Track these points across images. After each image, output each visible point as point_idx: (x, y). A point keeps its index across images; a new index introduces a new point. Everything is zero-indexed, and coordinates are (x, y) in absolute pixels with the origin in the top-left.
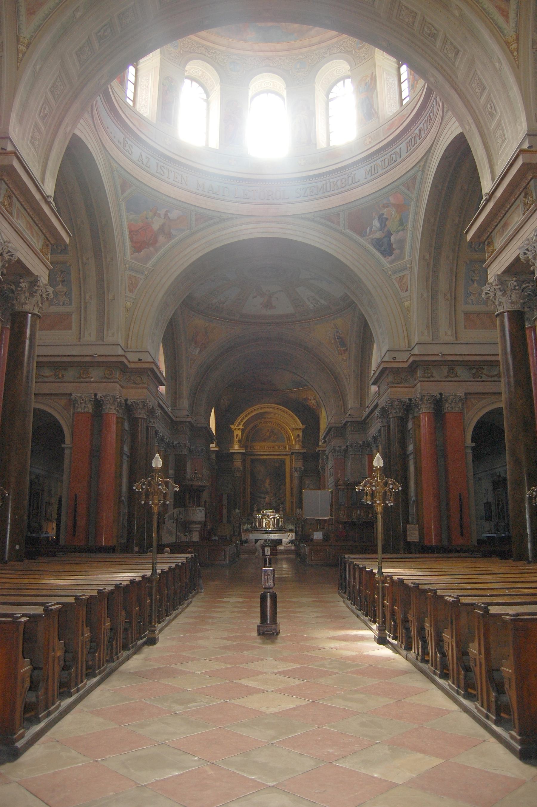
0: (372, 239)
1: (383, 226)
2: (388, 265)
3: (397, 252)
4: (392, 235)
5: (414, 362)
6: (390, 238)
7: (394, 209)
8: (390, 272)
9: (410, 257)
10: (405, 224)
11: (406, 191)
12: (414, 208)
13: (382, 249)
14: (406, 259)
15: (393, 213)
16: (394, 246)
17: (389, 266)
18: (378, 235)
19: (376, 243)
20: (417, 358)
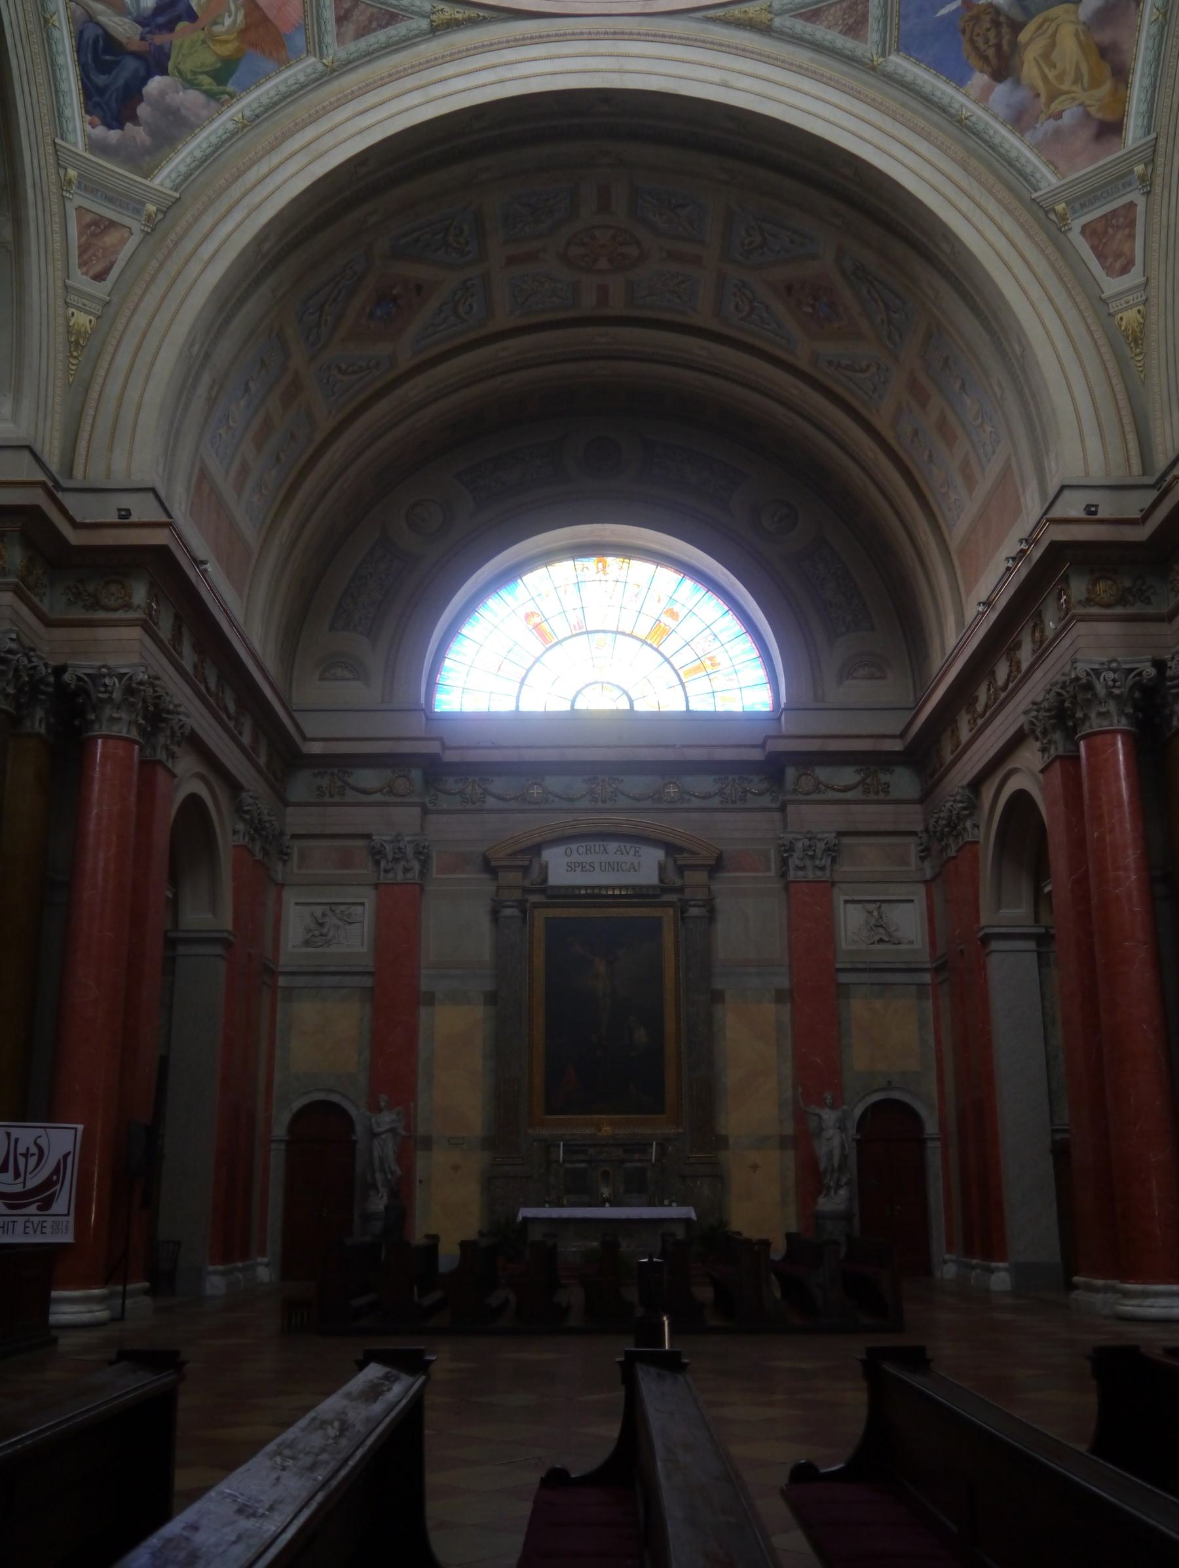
0: (91, 18)
1: (161, 20)
2: (80, 149)
3: (137, 133)
4: (164, 72)
5: (162, 554)
6: (149, 75)
7: (240, 17)
8: (72, 173)
9: (176, 190)
10: (230, 88)
11: (329, 14)
12: (302, 78)
13: (101, 80)
14: (156, 182)
15: (228, 21)
16: (143, 110)
17: (80, 149)
18: (123, 28)
19: (96, 41)
20: (174, 548)
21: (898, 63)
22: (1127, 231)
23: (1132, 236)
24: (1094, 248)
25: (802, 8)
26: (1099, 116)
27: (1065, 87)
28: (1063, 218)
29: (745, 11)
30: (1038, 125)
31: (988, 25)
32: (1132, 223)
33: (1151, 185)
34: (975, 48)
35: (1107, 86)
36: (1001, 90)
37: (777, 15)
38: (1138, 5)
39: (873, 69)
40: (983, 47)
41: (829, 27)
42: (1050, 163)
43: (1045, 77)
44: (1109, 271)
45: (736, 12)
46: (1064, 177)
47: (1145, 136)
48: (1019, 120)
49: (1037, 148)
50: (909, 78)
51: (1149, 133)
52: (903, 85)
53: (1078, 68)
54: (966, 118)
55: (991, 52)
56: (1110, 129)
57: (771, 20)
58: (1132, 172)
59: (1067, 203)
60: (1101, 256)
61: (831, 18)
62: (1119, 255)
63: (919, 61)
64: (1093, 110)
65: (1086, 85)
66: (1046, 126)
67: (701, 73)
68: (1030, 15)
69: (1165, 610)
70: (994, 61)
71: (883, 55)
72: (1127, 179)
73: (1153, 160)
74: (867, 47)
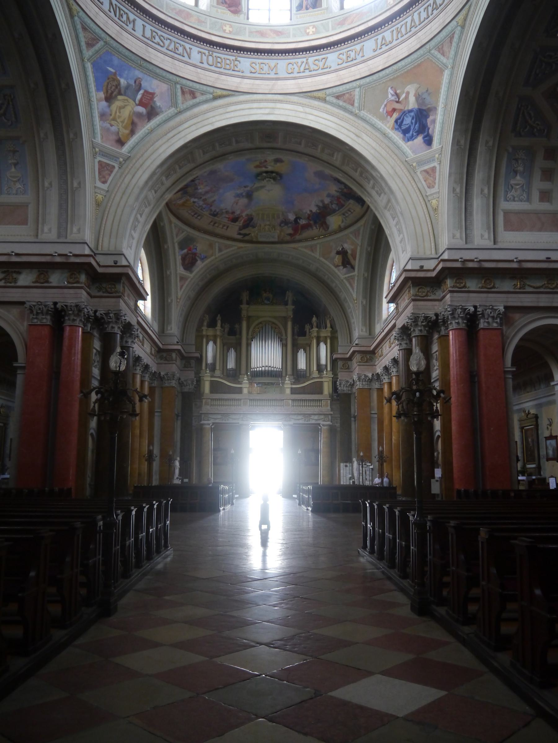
21: (89, 66)
22: (109, 172)
23: (110, 175)
24: (99, 169)
25: (84, 23)
26: (121, 136)
27: (119, 120)
28: (96, 153)
29: (73, 5)
30: (105, 122)
31: (114, 84)
32: (112, 172)
33: (122, 166)
34: (107, 86)
35: (127, 132)
36: (104, 103)
37: (78, 16)
38: (148, 122)
39: (83, 61)
40: (109, 88)
41: (84, 37)
42: (102, 135)
43: (116, 113)
44: (100, 179)
45: (71, 2)
46: (102, 143)
47: (127, 153)
48: (103, 116)
49: (102, 129)
50: (88, 74)
51: (129, 153)
52: (85, 75)
53: (125, 119)
54: (92, 101)
55: (110, 92)
56: (121, 142)
57: (76, 16)
58: (119, 159)
59: (99, 150)
60: (99, 173)
61: (87, 35)
62: (104, 177)
63: (93, 72)
64: (120, 133)
65: (123, 126)
66: (107, 125)
67: (60, 14)
68: (125, 94)
69: (93, 294)
70: (108, 95)
71: (88, 60)
72: (117, 159)
73: (125, 161)
74: (88, 53)
